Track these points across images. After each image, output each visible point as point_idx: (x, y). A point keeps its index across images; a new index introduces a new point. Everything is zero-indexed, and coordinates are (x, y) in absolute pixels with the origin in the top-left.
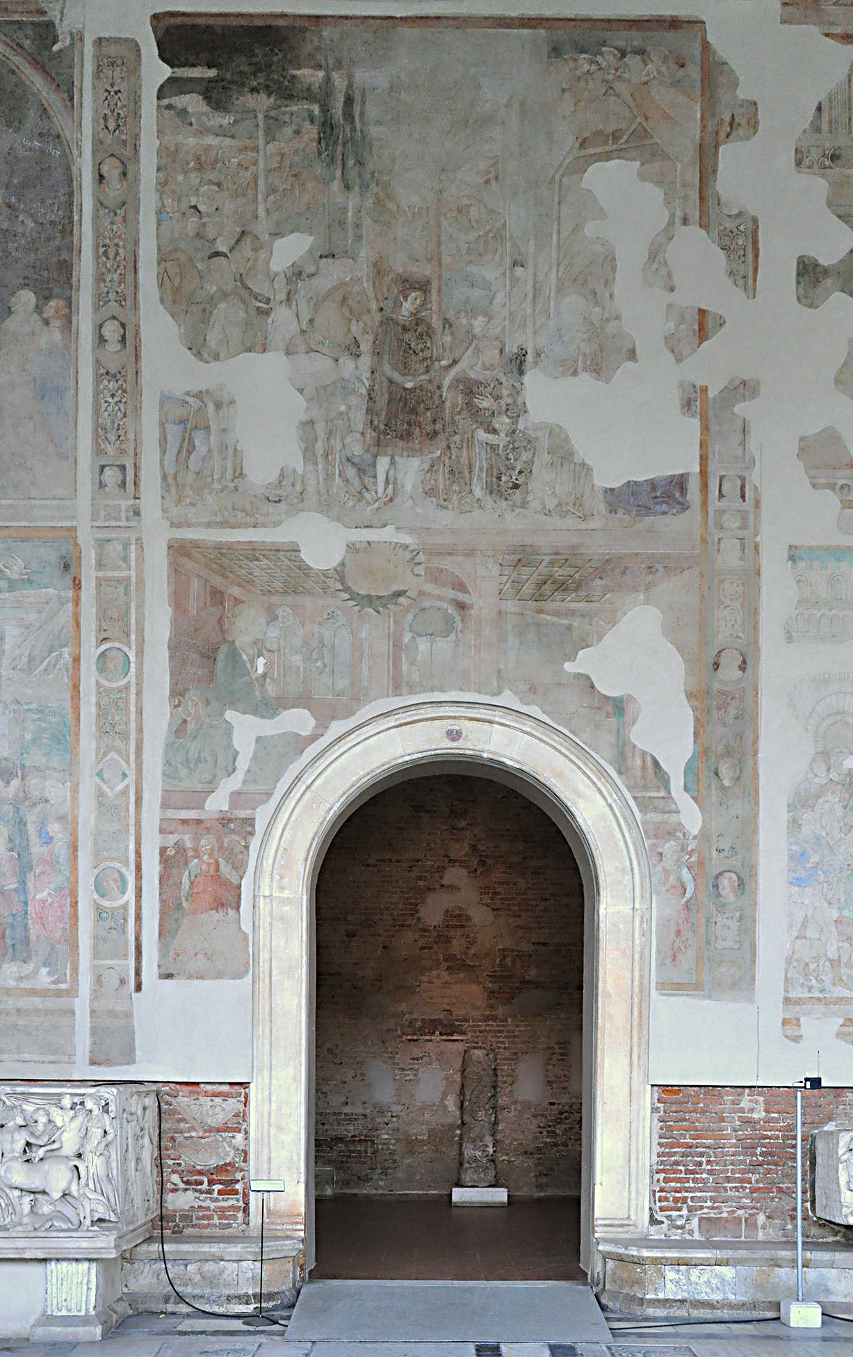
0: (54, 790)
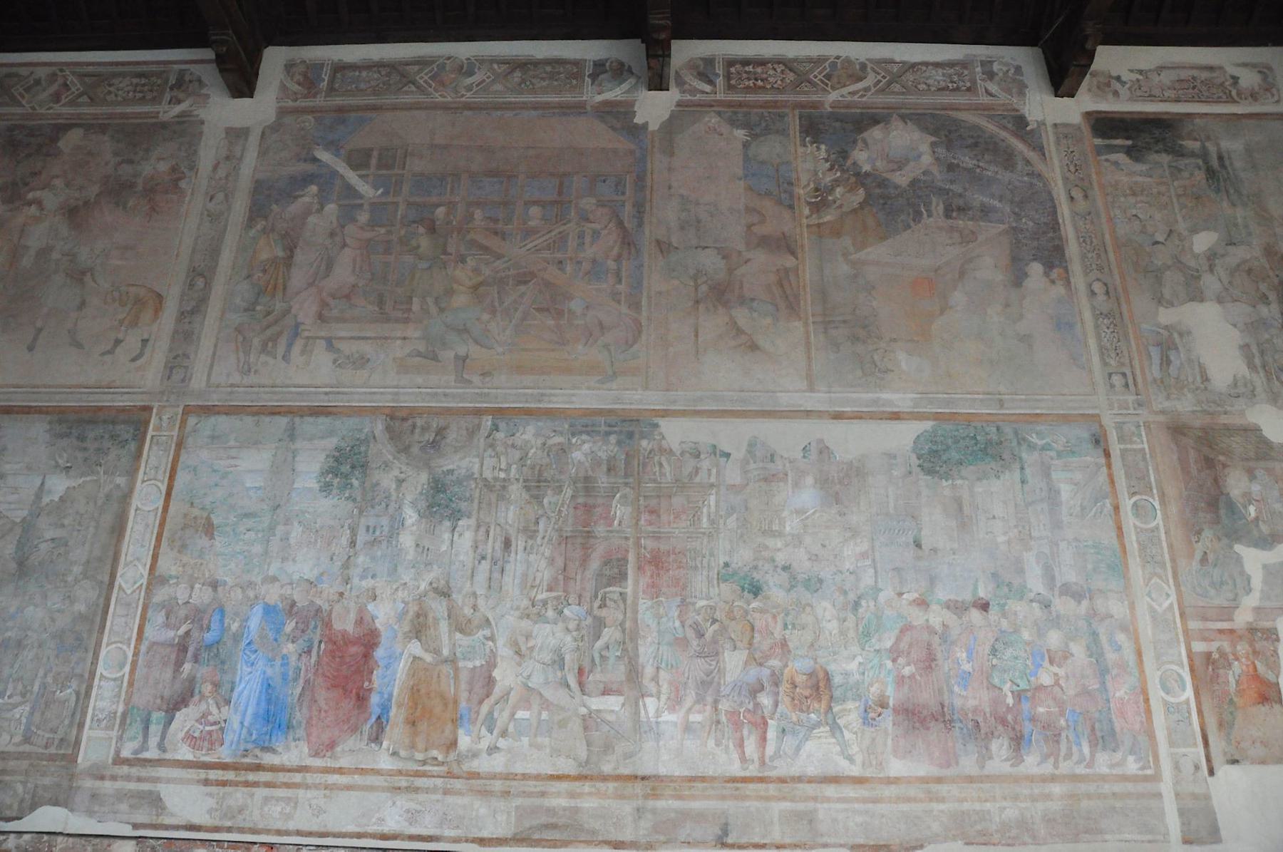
0: (1117, 608)
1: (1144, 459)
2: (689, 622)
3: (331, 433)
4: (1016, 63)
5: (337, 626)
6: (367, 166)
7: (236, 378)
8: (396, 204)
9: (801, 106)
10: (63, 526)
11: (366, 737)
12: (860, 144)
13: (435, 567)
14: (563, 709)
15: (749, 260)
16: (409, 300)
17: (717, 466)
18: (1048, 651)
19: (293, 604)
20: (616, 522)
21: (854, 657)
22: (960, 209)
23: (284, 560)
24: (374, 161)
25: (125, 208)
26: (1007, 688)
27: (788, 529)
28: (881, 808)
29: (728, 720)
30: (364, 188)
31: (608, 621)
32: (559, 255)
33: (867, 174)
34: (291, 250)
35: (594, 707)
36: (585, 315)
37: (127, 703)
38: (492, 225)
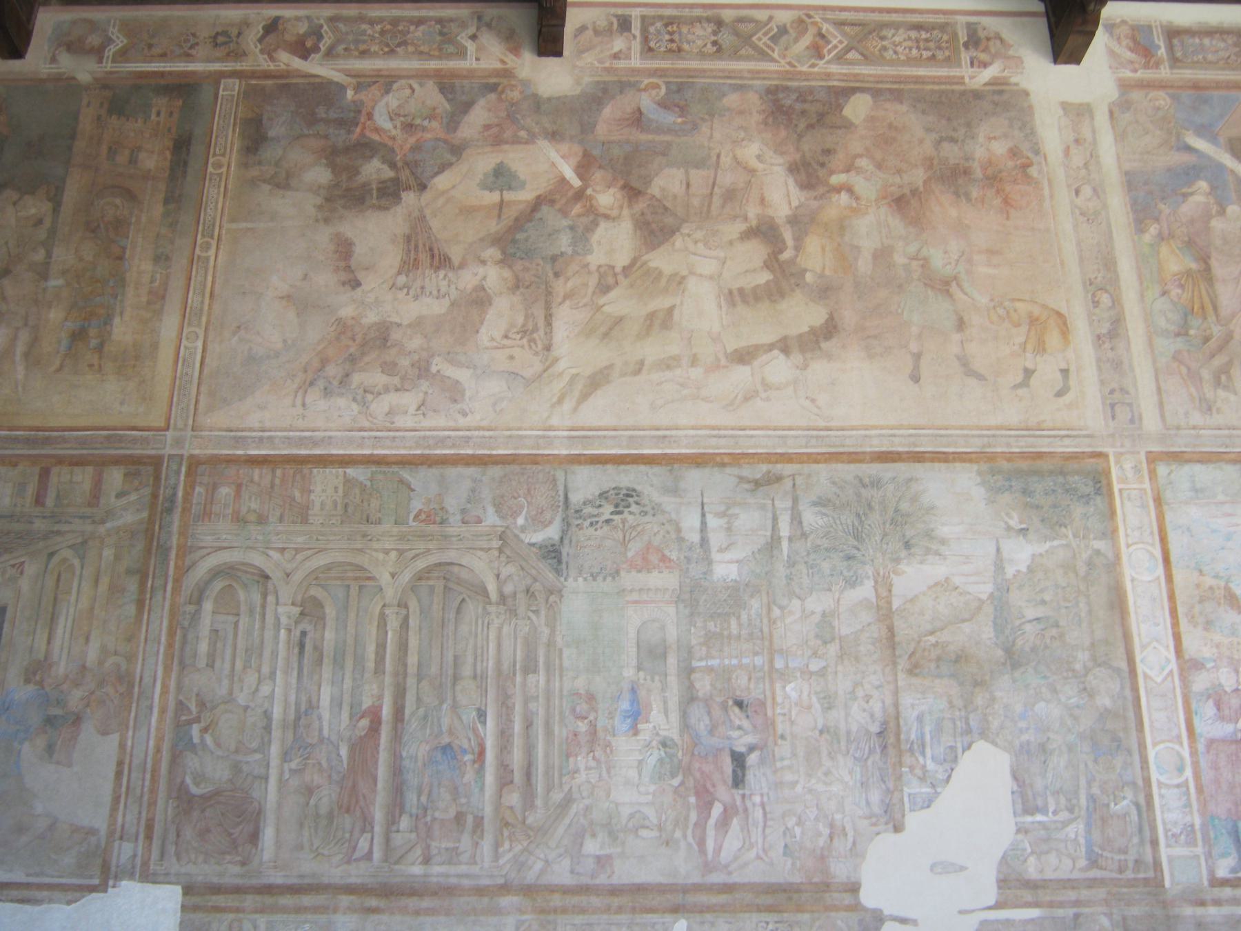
7: (1197, 418)
10: (1043, 602)
25: (969, 199)
37: (1203, 812)
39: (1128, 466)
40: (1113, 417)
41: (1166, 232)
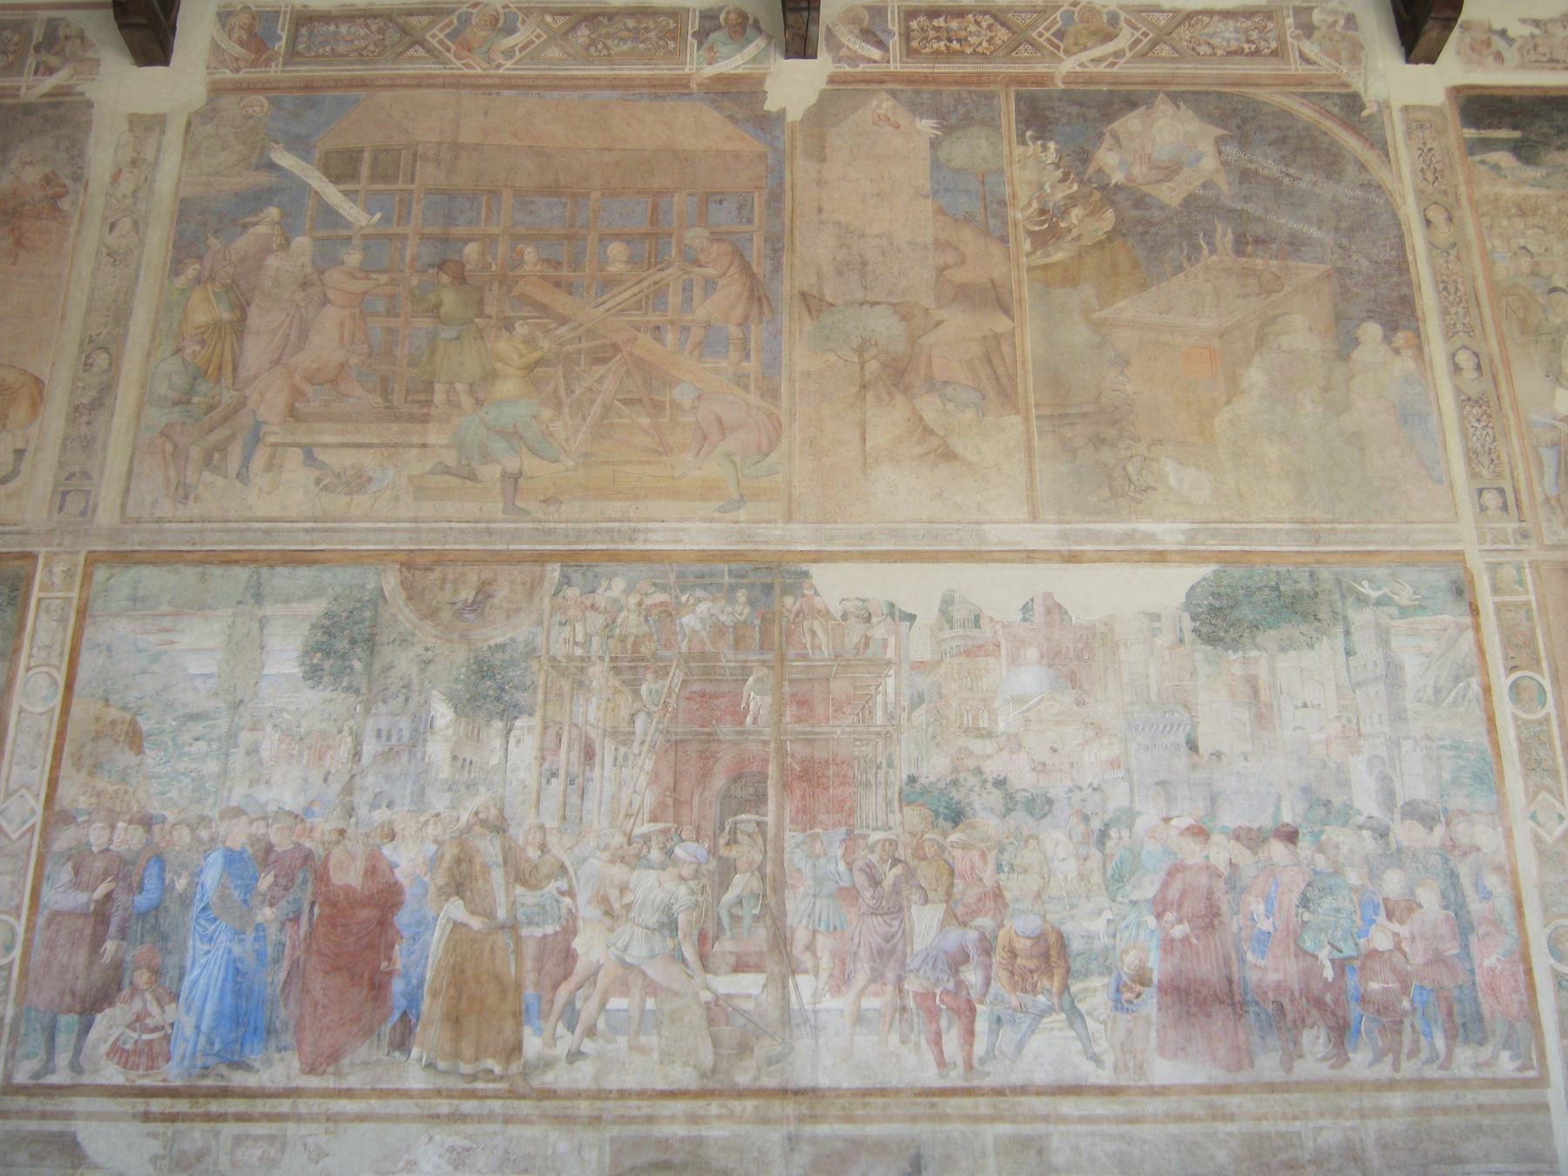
0: (1485, 836)
1: (1529, 618)
2: (860, 863)
3: (319, 591)
4: (1347, 10)
5: (338, 878)
6: (354, 176)
7: (166, 508)
8: (404, 237)
9: (1019, 81)
11: (386, 1041)
12: (1108, 141)
13: (482, 789)
14: (676, 993)
15: (939, 323)
16: (429, 387)
17: (897, 634)
18: (1386, 900)
19: (269, 848)
20: (749, 719)
21: (1100, 912)
22: (1258, 241)
23: (253, 783)
24: (365, 170)
26: (1324, 954)
27: (1001, 726)
28: (1144, 1130)
29: (919, 1006)
30: (352, 212)
31: (741, 865)
32: (654, 318)
33: (1118, 188)
34: (242, 308)
35: (722, 991)
36: (694, 408)
38: (551, 272)
39: (58, 569)
40: (61, 509)
41: (207, 274)
